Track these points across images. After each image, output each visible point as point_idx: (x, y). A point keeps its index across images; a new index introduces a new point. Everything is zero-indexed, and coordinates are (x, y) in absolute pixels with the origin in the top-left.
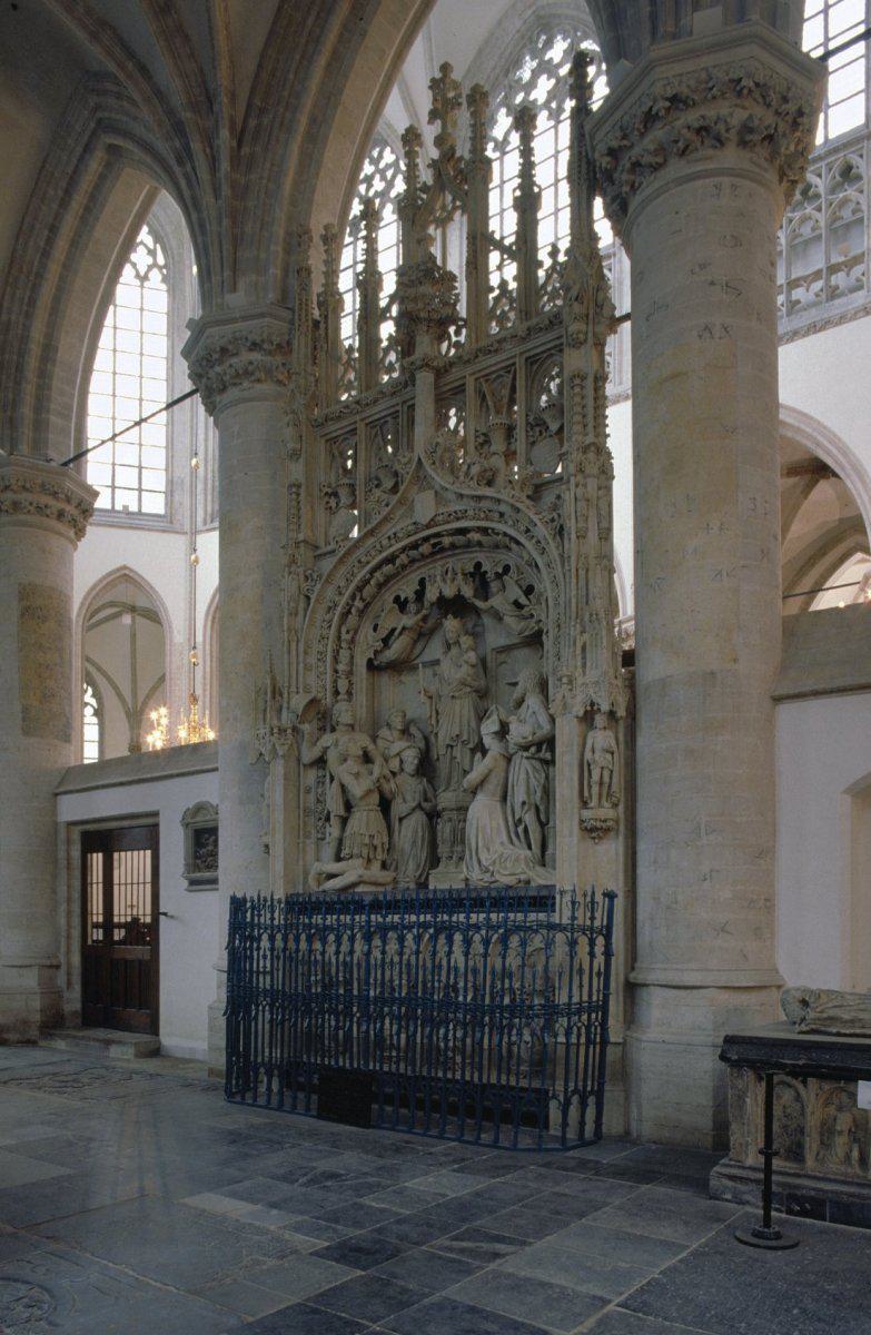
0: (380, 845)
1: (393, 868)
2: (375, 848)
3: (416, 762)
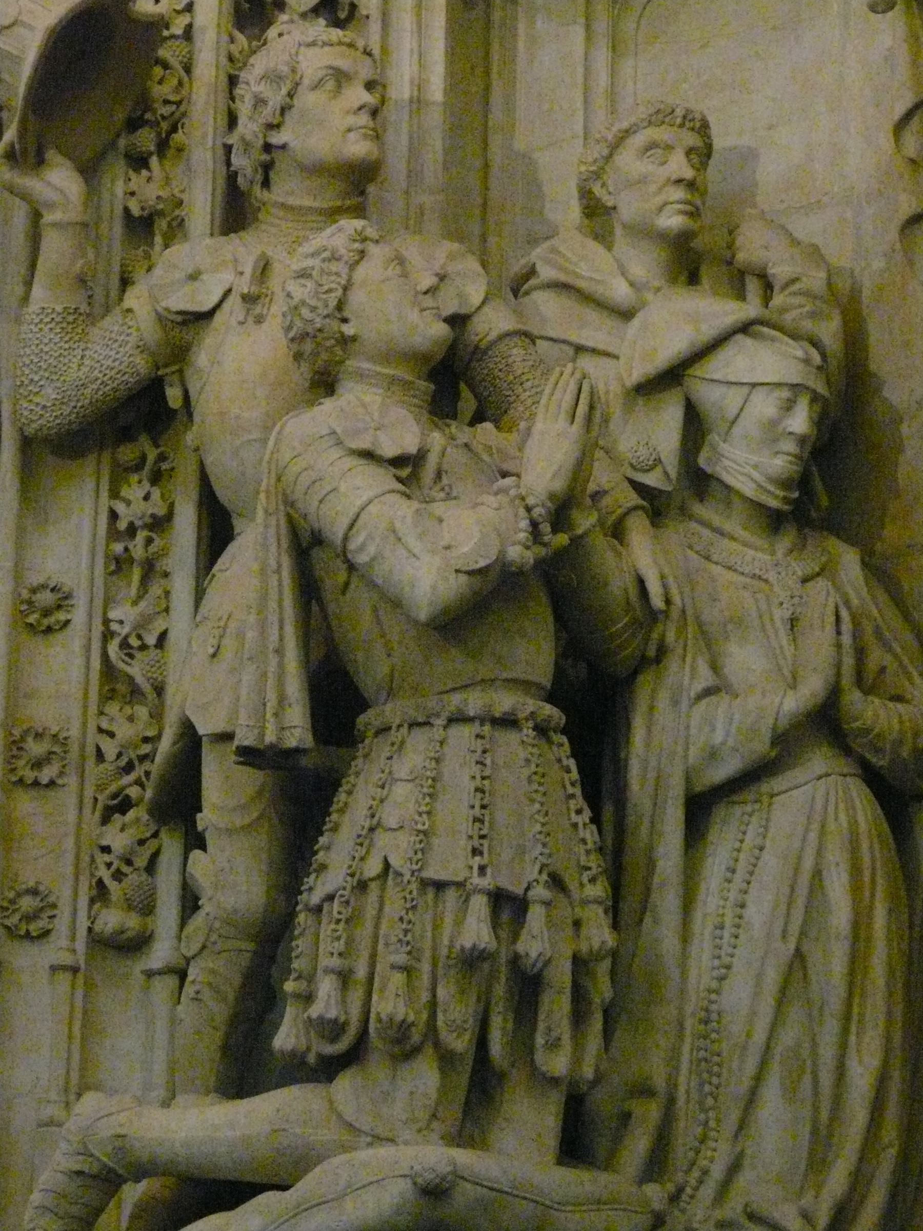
0: (561, 975)
1: (638, 1145)
2: (528, 986)
3: (800, 421)
